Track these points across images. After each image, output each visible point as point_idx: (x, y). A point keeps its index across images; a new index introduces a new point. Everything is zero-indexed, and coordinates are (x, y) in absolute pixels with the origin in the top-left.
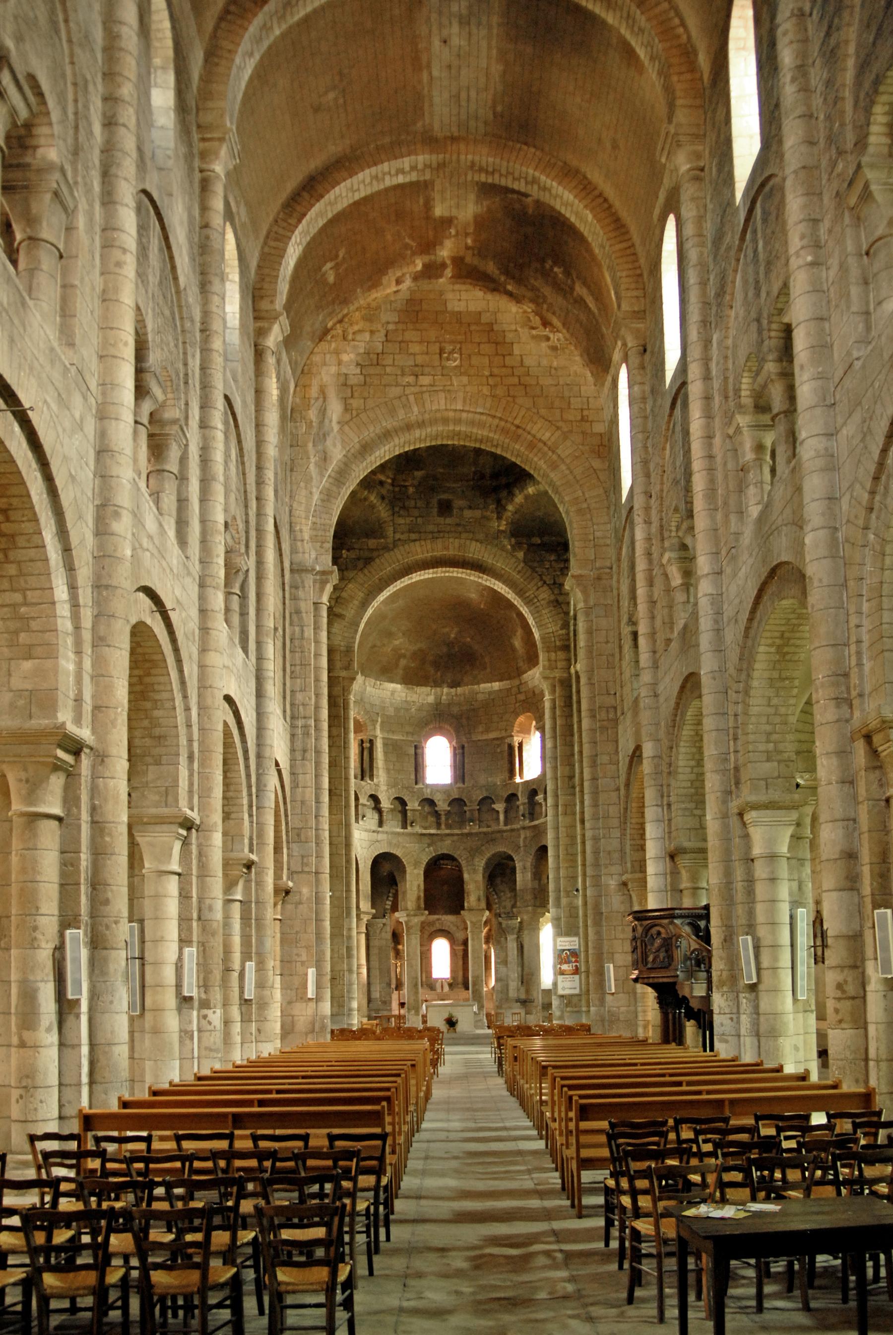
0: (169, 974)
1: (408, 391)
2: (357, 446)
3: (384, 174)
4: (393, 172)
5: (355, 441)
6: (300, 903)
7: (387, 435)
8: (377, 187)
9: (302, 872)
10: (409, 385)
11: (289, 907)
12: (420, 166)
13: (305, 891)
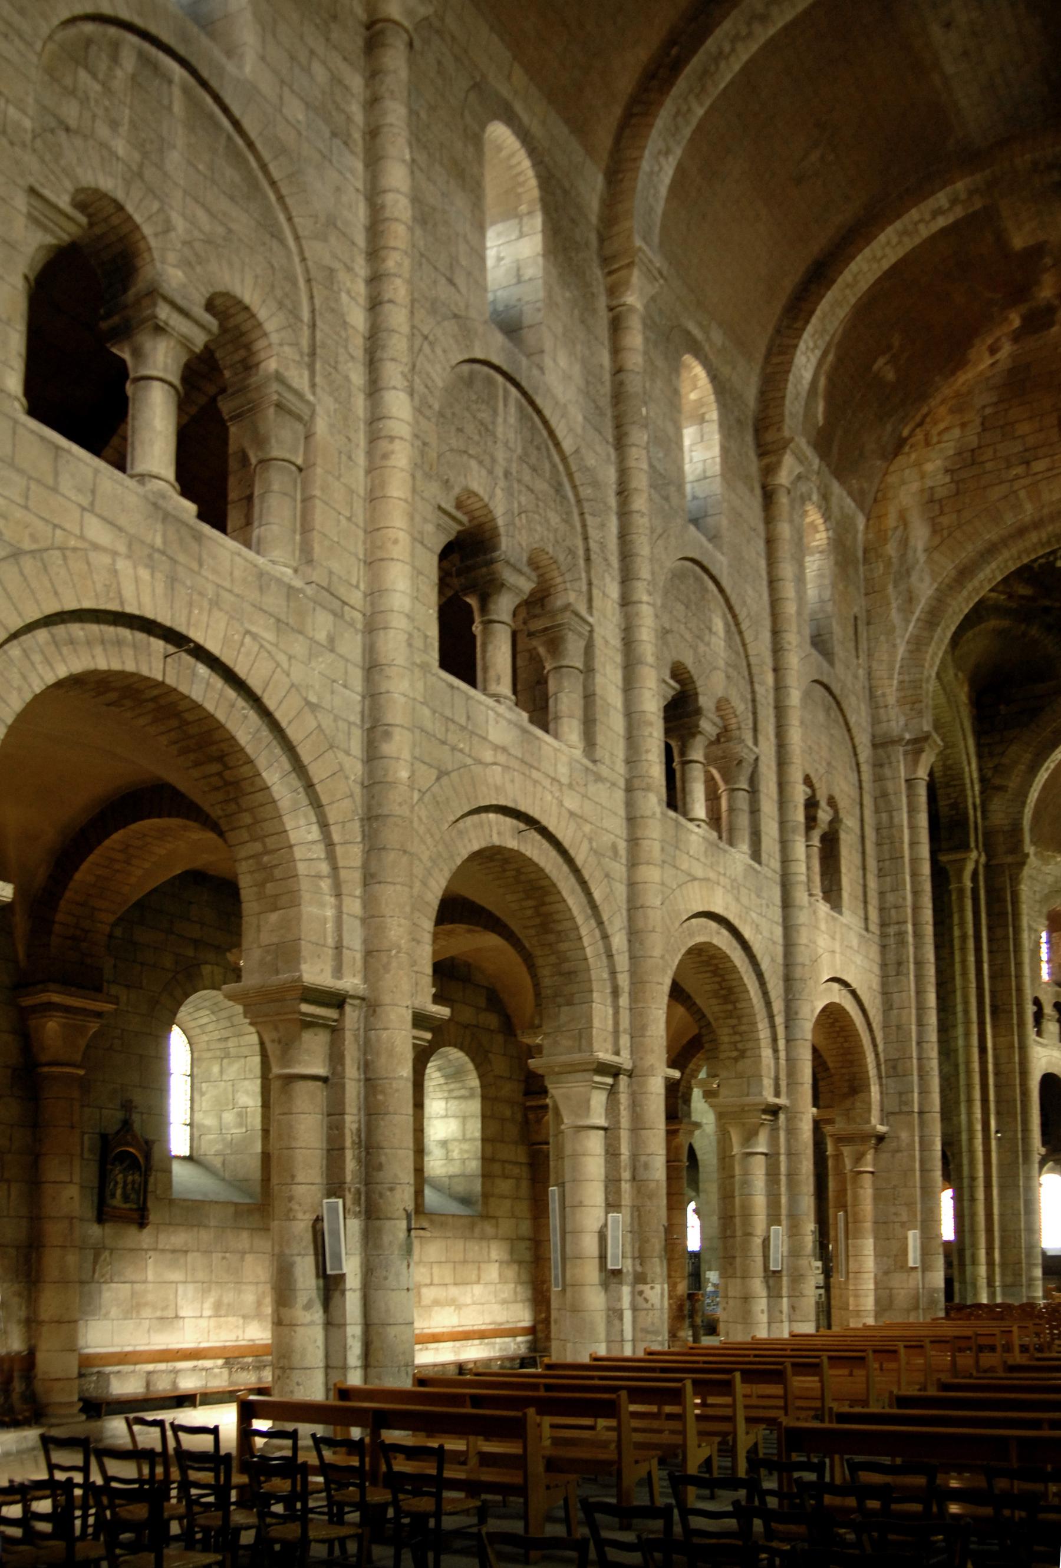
0: (590, 1245)
1: (1017, 485)
2: (953, 573)
3: (916, 224)
4: (927, 217)
5: (949, 568)
6: (898, 1150)
7: (991, 551)
8: (909, 244)
9: (900, 1113)
10: (1017, 477)
11: (884, 1156)
12: (963, 196)
13: (904, 1135)
